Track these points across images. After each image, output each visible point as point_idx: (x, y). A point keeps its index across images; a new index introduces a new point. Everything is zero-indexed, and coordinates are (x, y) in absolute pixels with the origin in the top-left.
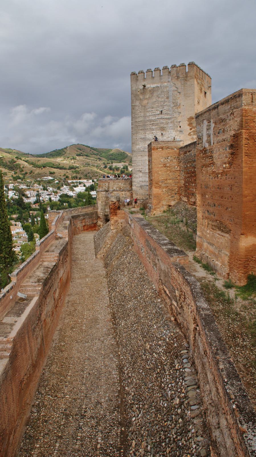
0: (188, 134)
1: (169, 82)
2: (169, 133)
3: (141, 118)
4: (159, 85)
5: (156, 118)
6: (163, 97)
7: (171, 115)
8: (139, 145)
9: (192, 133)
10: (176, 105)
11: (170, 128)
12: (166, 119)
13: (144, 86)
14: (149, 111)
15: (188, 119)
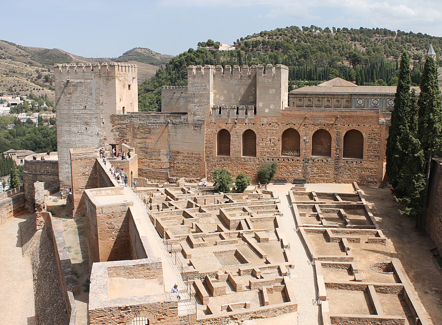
0: (110, 130)
1: (92, 79)
2: (93, 128)
3: (65, 111)
4: (82, 81)
5: (81, 112)
6: (86, 94)
7: (94, 112)
8: (64, 138)
9: (114, 130)
10: (99, 102)
11: (94, 123)
12: (90, 114)
13: (68, 81)
14: (74, 105)
15: (110, 116)
